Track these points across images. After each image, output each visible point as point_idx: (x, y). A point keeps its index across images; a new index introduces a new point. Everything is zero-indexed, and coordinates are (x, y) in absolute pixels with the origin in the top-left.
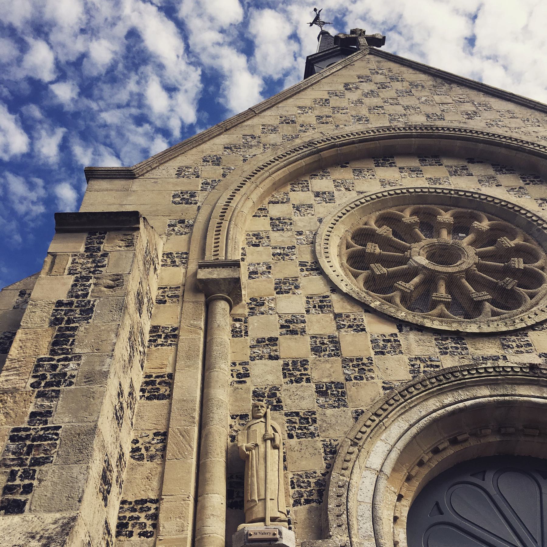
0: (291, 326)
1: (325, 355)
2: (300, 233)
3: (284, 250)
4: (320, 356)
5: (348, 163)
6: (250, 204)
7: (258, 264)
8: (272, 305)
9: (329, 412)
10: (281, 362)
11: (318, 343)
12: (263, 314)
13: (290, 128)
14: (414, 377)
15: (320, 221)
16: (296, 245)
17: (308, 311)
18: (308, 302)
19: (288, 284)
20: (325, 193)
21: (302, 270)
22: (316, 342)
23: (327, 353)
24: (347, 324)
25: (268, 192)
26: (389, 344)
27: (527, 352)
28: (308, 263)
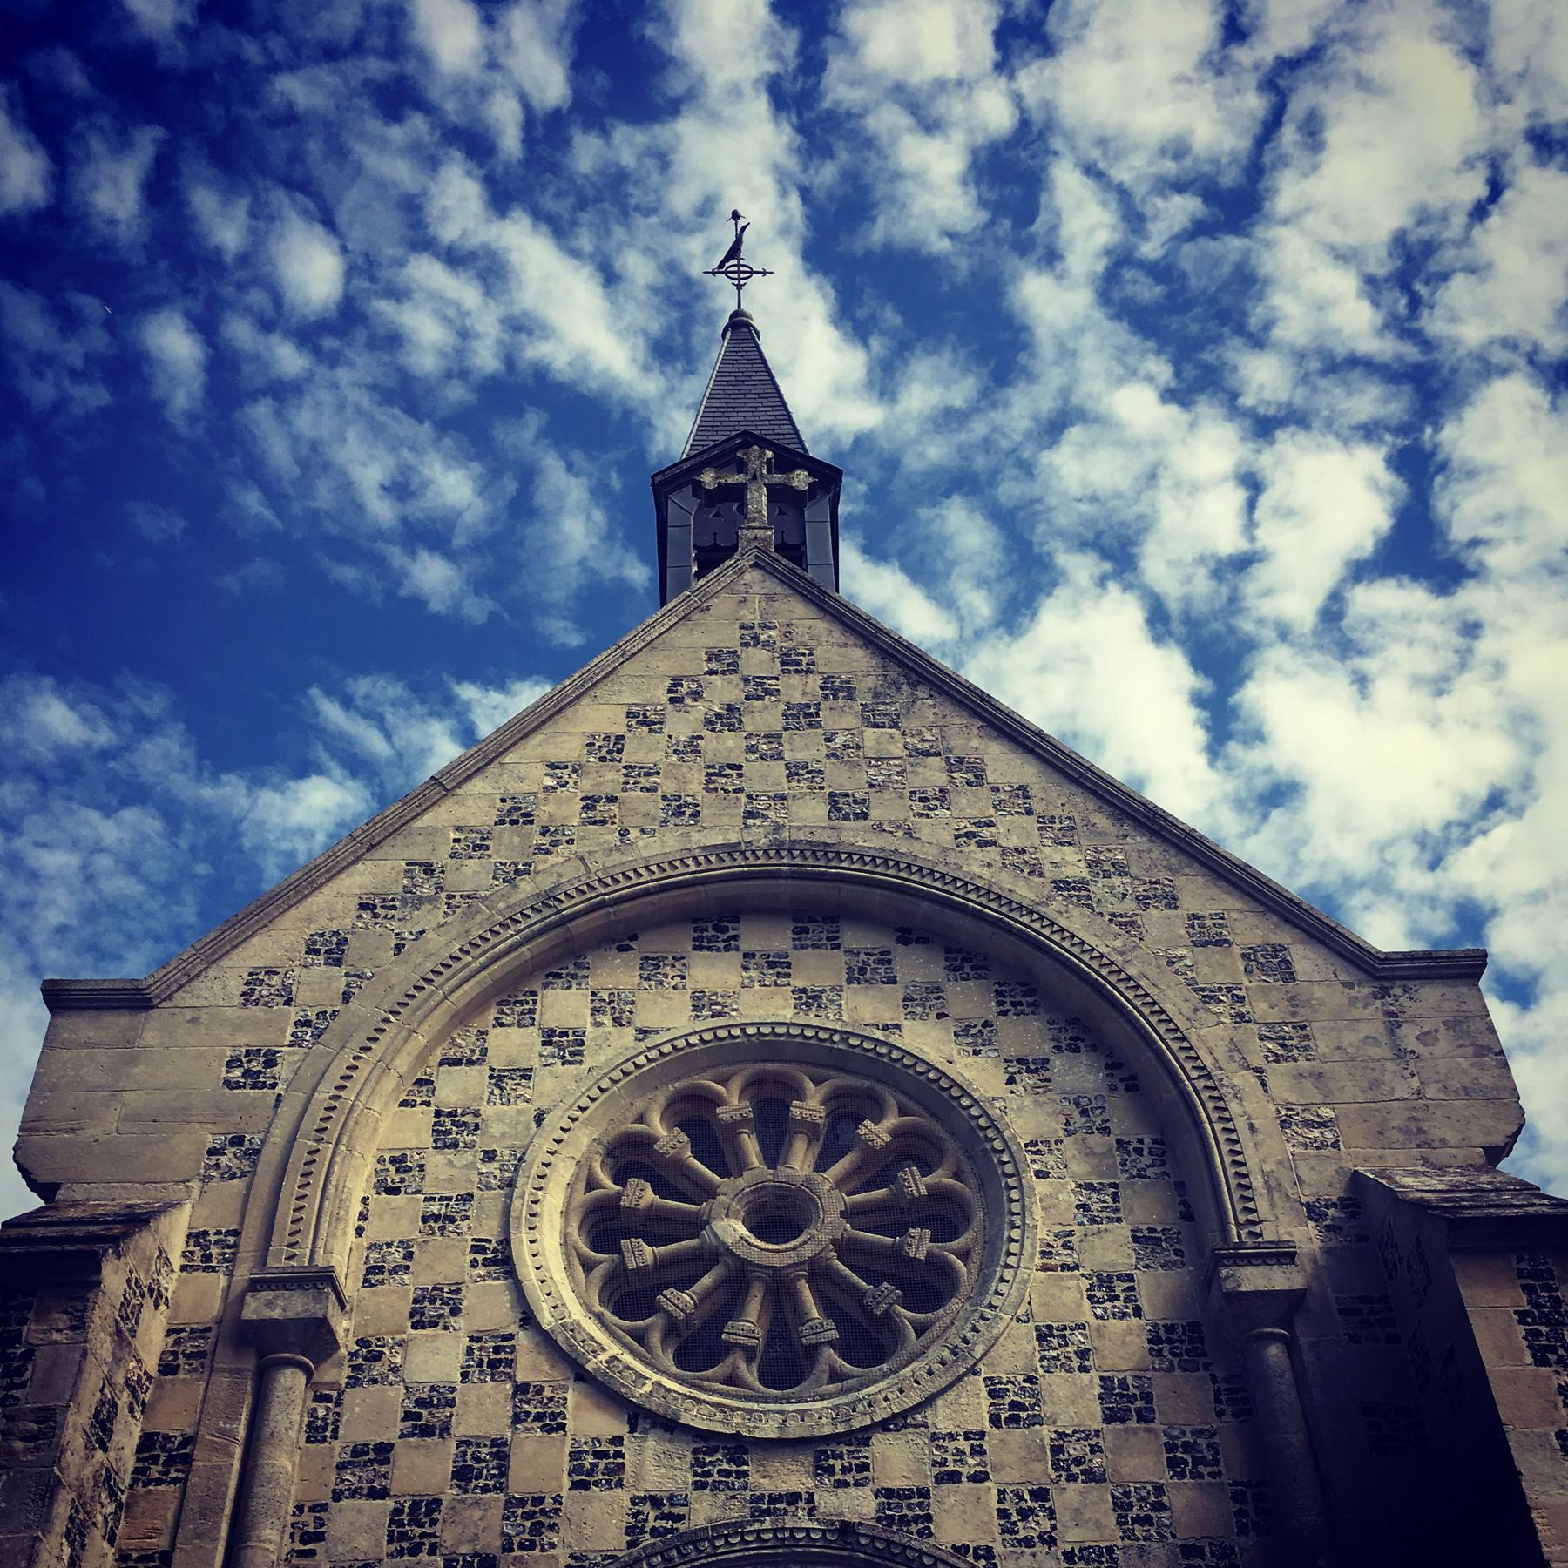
0: (424, 1412)
1: (476, 1487)
2: (490, 1156)
3: (448, 1205)
4: (466, 1491)
5: (634, 938)
6: (390, 1082)
7: (389, 1245)
8: (398, 1360)
10: (390, 1504)
11: (469, 1457)
12: (375, 1381)
13: (516, 840)
14: (631, 1545)
15: (539, 1119)
16: (476, 1192)
17: (465, 1375)
18: (470, 1351)
19: (438, 1303)
20: (564, 1034)
21: (474, 1263)
22: (465, 1454)
23: (481, 1482)
24: (534, 1411)
25: (444, 1035)
26: (602, 1464)
27: (857, 1484)
28: (489, 1241)
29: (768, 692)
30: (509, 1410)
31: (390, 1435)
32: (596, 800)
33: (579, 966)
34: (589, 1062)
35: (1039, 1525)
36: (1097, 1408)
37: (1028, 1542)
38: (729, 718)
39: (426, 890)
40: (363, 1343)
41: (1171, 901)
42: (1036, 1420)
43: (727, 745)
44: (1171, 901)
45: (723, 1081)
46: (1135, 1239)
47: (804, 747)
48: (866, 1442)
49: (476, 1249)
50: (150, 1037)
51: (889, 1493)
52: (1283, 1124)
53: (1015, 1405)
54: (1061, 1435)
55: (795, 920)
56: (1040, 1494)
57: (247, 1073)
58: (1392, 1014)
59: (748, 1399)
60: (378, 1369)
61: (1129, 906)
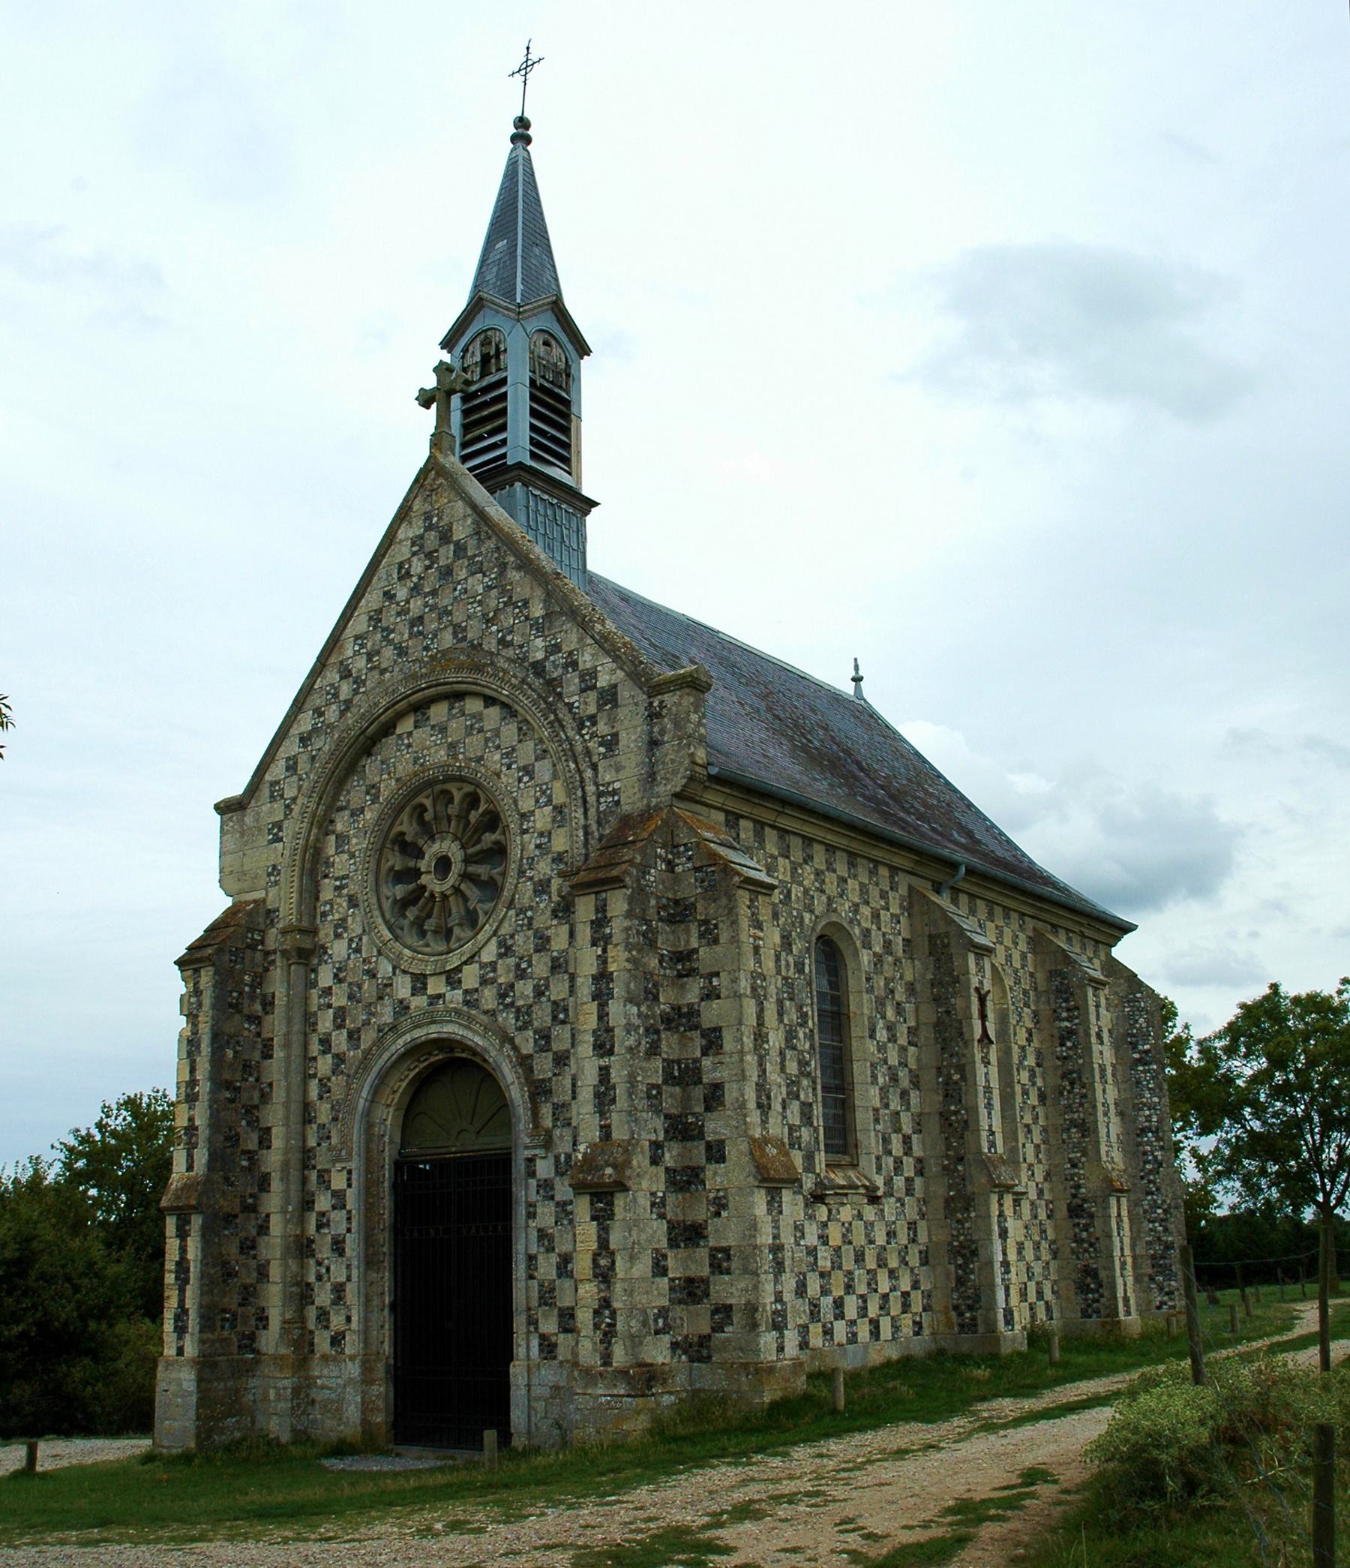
35: (508, 1000)
43: (416, 606)
45: (427, 797)
48: (461, 971)
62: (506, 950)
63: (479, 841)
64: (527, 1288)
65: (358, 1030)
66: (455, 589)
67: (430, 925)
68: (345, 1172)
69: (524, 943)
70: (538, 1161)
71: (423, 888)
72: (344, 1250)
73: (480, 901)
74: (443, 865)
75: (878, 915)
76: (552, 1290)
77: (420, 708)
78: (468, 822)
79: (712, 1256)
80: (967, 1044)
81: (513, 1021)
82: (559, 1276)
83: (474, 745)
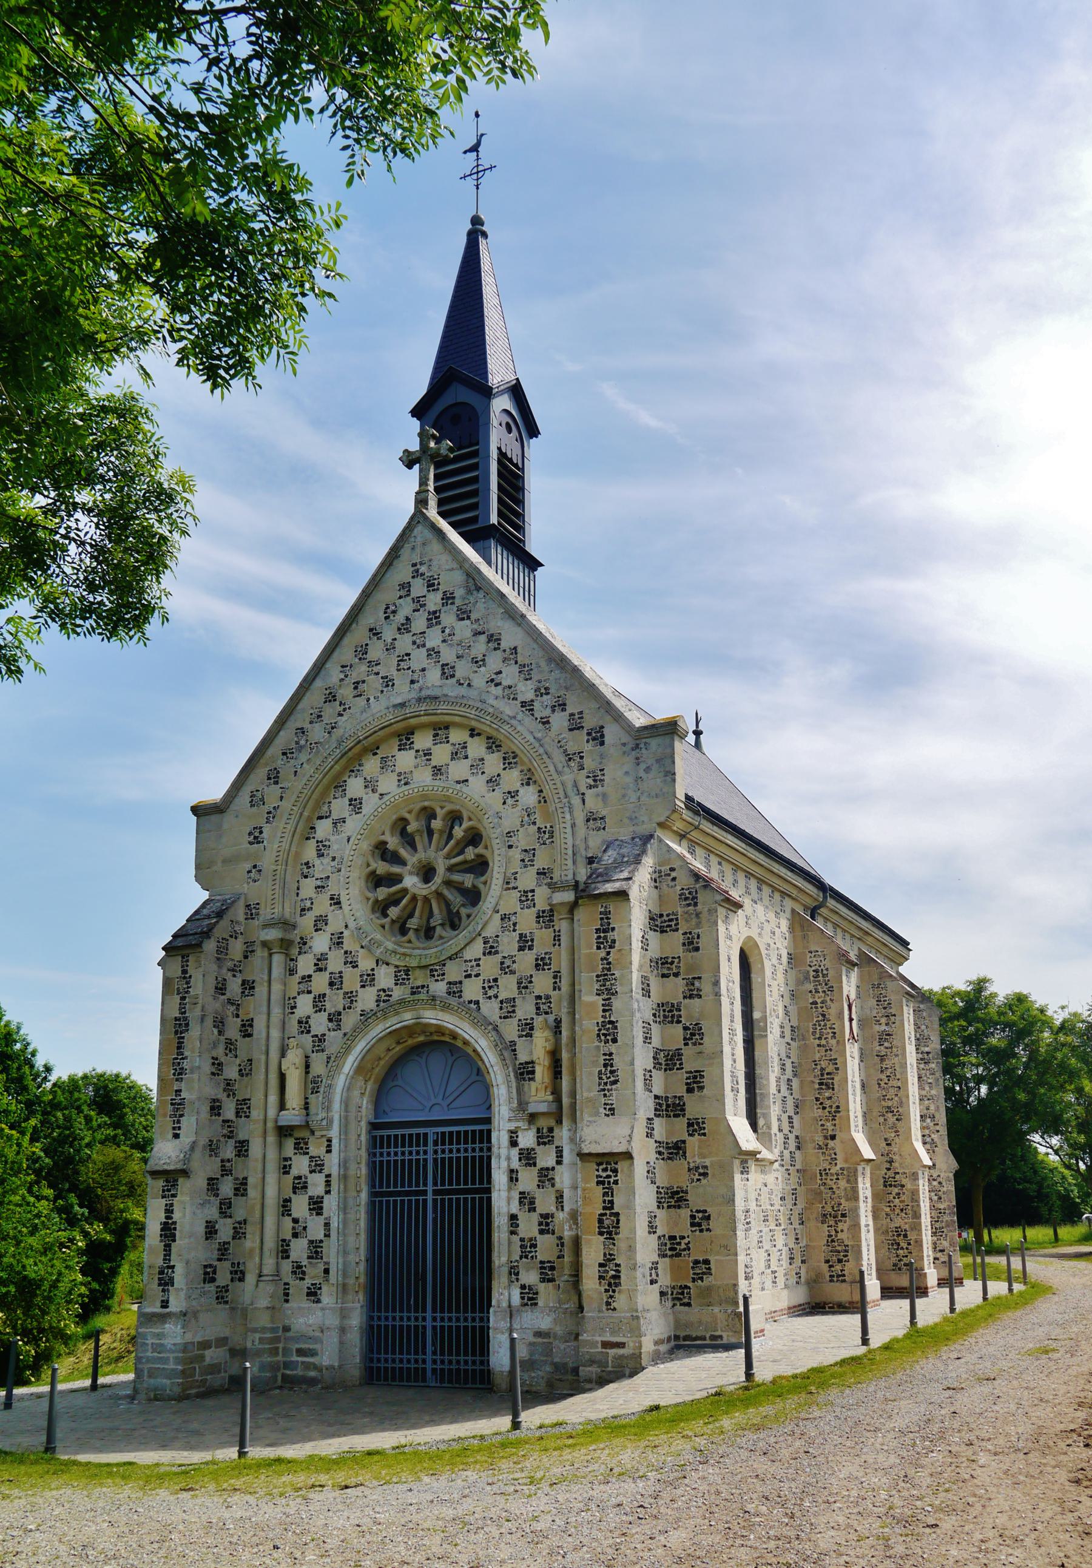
5: (378, 748)
9: (332, 1033)
10: (312, 996)
29: (421, 606)
30: (343, 960)
31: (311, 972)
32: (358, 683)
33: (360, 765)
34: (364, 811)
35: (491, 993)
36: (517, 945)
37: (490, 998)
38: (405, 627)
39: (302, 742)
40: (302, 938)
41: (563, 706)
42: (497, 952)
43: (404, 643)
44: (563, 706)
45: (410, 812)
46: (538, 873)
47: (434, 639)
48: (444, 965)
49: (332, 899)
50: (226, 826)
51: (450, 983)
52: (588, 820)
53: (492, 947)
54: (504, 957)
55: (435, 729)
56: (496, 980)
57: (255, 838)
58: (637, 758)
59: (414, 949)
60: (307, 946)
61: (547, 712)
62: (491, 950)
63: (462, 852)
64: (510, 1243)
65: (339, 1014)
66: (443, 632)
67: (413, 923)
68: (325, 1139)
69: (508, 944)
70: (520, 1134)
71: (405, 891)
72: (321, 1208)
73: (463, 905)
74: (427, 873)
75: (774, 933)
76: (535, 1246)
77: (405, 737)
78: (450, 836)
79: (693, 1217)
80: (841, 1043)
81: (498, 1010)
82: (541, 1232)
83: (459, 769)
